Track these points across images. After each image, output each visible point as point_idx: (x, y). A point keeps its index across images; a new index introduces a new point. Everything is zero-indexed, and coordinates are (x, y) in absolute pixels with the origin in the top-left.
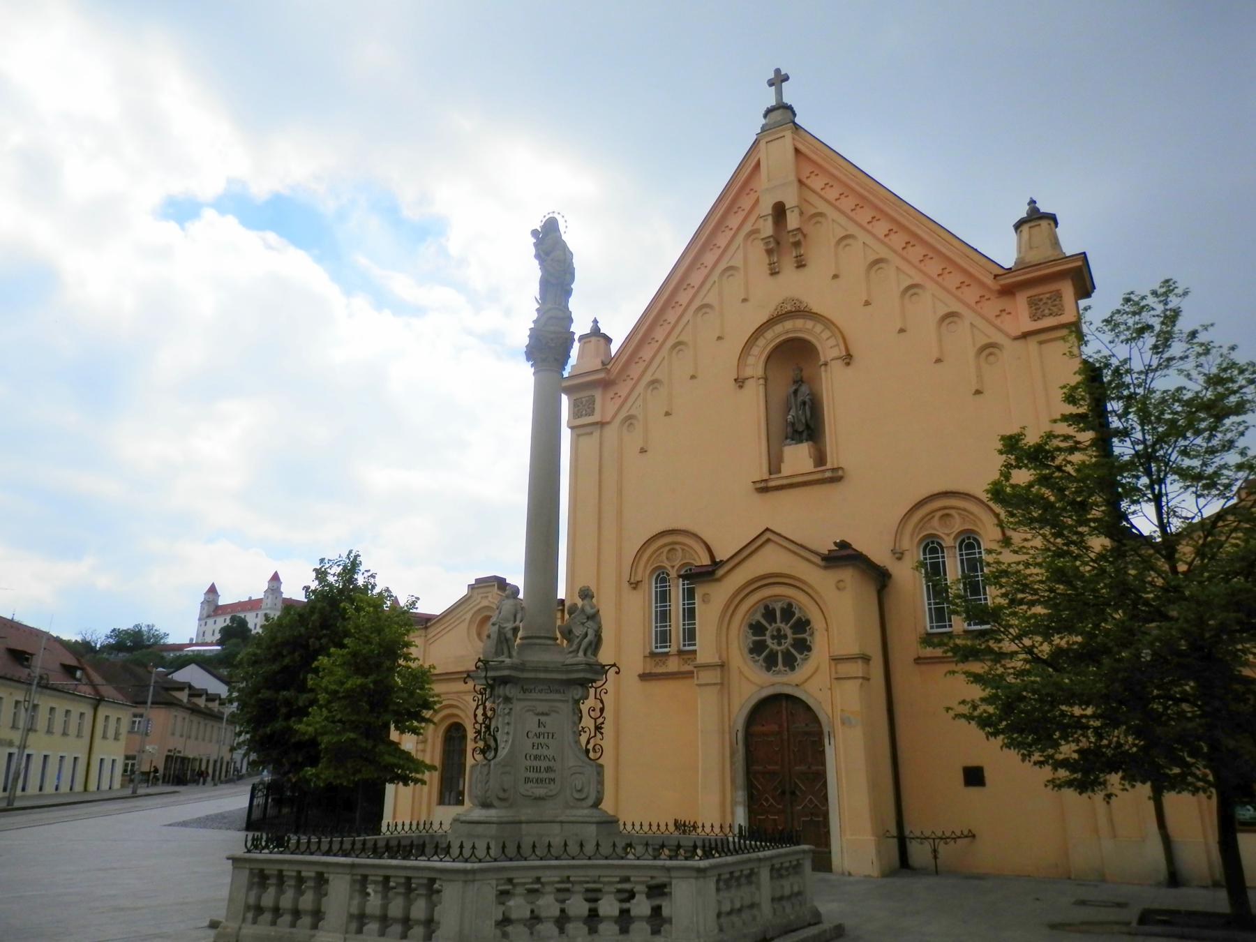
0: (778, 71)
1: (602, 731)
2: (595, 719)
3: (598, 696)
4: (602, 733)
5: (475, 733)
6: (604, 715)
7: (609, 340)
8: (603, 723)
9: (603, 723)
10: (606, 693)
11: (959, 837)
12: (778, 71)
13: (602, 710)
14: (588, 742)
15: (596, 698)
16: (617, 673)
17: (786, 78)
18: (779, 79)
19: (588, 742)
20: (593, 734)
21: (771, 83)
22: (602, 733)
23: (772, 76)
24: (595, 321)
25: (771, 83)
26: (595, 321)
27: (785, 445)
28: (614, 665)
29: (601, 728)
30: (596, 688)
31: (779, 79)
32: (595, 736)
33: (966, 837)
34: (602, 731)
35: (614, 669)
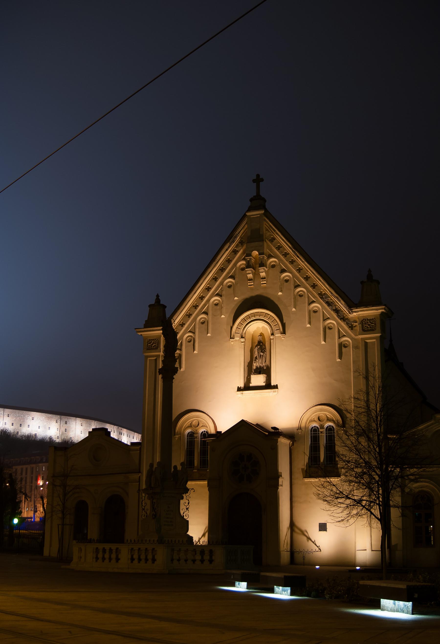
0: (258, 176)
1: (188, 510)
2: (186, 506)
3: (187, 499)
4: (188, 511)
5: (143, 509)
6: (189, 505)
7: (165, 307)
8: (189, 507)
9: (189, 507)
10: (190, 498)
11: (314, 552)
12: (258, 176)
13: (189, 503)
14: (184, 513)
15: (186, 499)
16: (194, 491)
17: (262, 180)
18: (258, 180)
19: (184, 513)
20: (185, 511)
21: (254, 181)
22: (188, 511)
23: (255, 178)
24: (158, 296)
25: (254, 181)
26: (158, 296)
27: (252, 374)
28: (193, 489)
29: (188, 509)
30: (186, 496)
31: (258, 180)
32: (186, 511)
33: (318, 551)
34: (188, 510)
35: (193, 490)
